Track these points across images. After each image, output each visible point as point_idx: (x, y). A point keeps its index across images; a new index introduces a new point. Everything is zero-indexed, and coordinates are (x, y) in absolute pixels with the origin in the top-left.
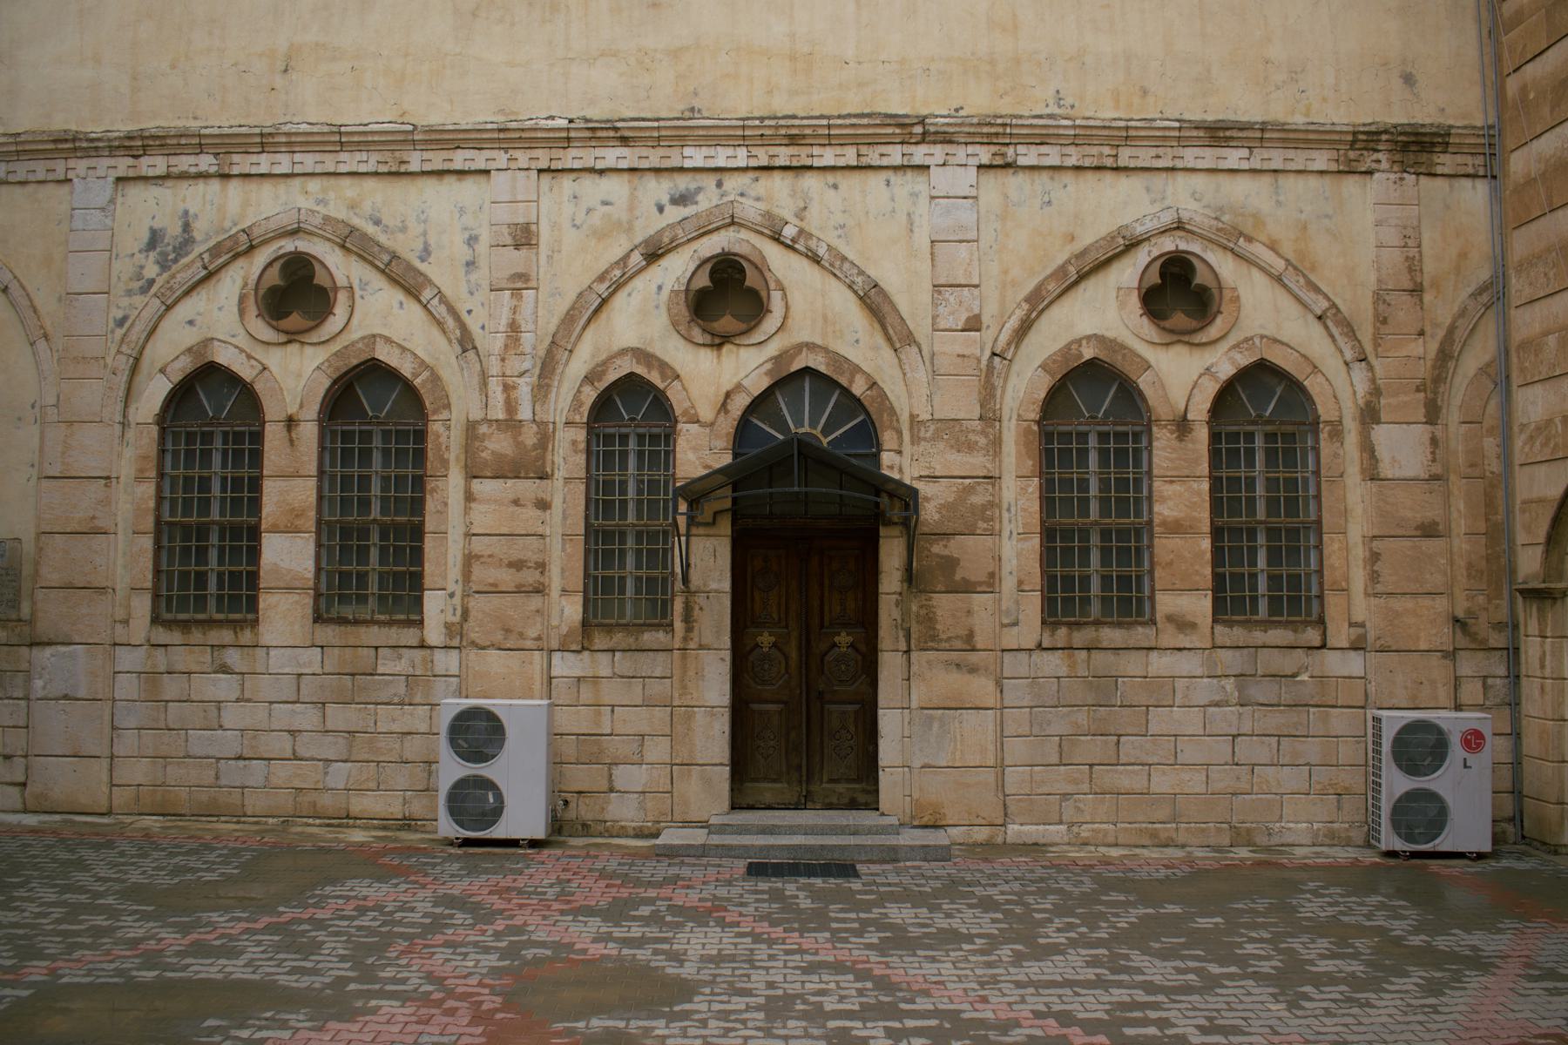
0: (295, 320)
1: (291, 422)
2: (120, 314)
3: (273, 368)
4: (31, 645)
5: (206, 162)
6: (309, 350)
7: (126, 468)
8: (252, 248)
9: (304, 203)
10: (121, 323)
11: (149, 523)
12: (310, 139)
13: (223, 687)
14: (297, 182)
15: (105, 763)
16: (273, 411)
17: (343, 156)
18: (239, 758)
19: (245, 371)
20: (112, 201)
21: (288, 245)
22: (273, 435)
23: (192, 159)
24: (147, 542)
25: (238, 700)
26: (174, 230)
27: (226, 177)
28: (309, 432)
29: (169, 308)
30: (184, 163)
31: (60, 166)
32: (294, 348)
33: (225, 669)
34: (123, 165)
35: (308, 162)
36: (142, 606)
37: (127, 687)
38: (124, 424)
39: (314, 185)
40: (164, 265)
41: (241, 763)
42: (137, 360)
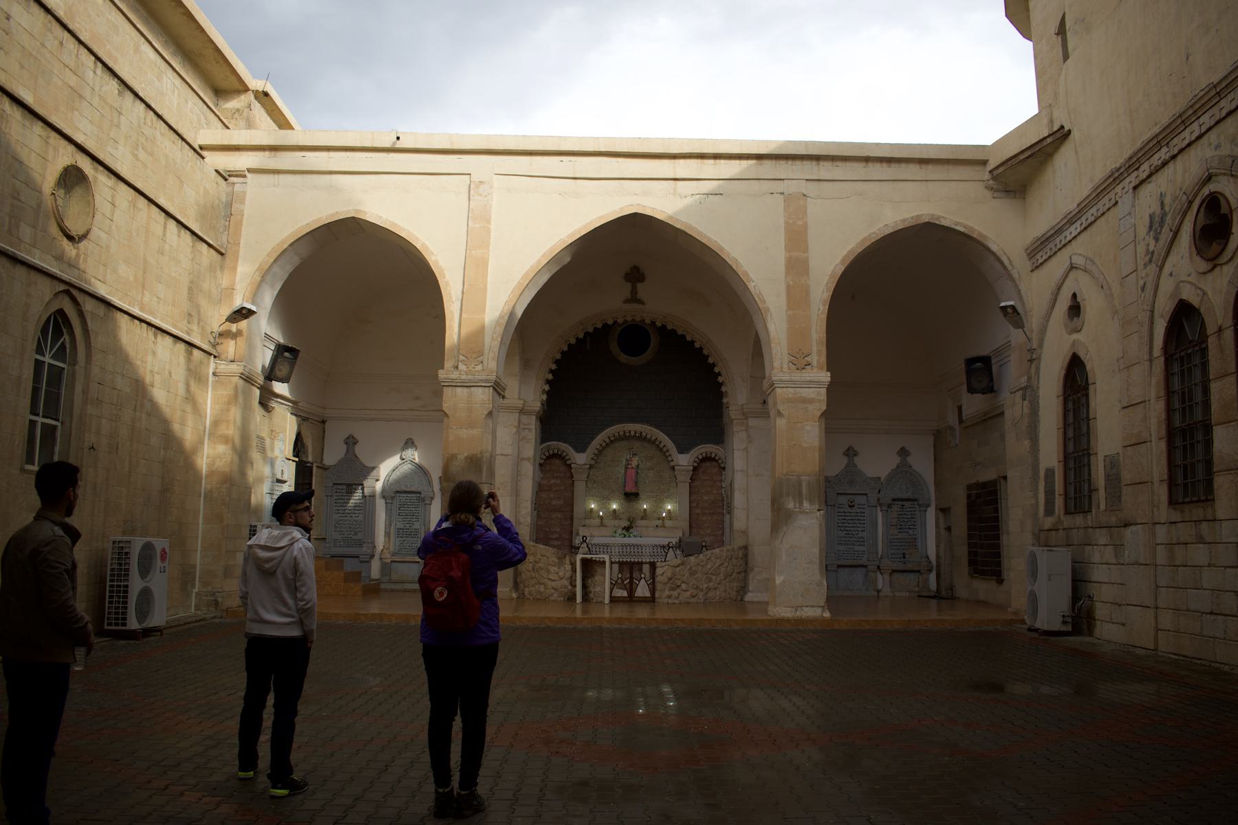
0: (1215, 247)
1: (1220, 330)
2: (1141, 283)
3: (1210, 293)
4: (1126, 526)
5: (1164, 154)
6: (1225, 268)
7: (1153, 395)
8: (1191, 203)
9: (1209, 153)
10: (1143, 289)
11: (1163, 432)
12: (1203, 101)
13: (1199, 554)
14: (1205, 139)
15: (1152, 611)
16: (1211, 329)
17: (1223, 103)
18: (1211, 613)
19: (1195, 301)
20: (1133, 206)
21: (1206, 191)
22: (1212, 342)
23: (1157, 156)
24: (1163, 445)
25: (1209, 565)
26: (1158, 211)
27: (1174, 157)
28: (1229, 335)
29: (1161, 268)
30: (1156, 160)
31: (1112, 195)
32: (1217, 270)
33: (1201, 540)
34: (1132, 179)
35: (1206, 120)
36: (1162, 492)
37: (1161, 556)
38: (1151, 361)
39: (1212, 135)
40: (1157, 239)
41: (1213, 617)
42: (1152, 312)
